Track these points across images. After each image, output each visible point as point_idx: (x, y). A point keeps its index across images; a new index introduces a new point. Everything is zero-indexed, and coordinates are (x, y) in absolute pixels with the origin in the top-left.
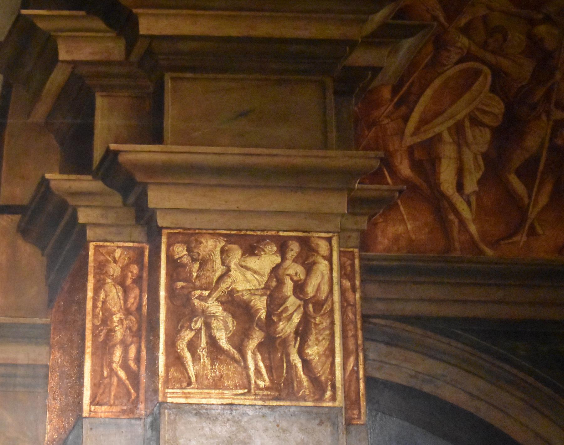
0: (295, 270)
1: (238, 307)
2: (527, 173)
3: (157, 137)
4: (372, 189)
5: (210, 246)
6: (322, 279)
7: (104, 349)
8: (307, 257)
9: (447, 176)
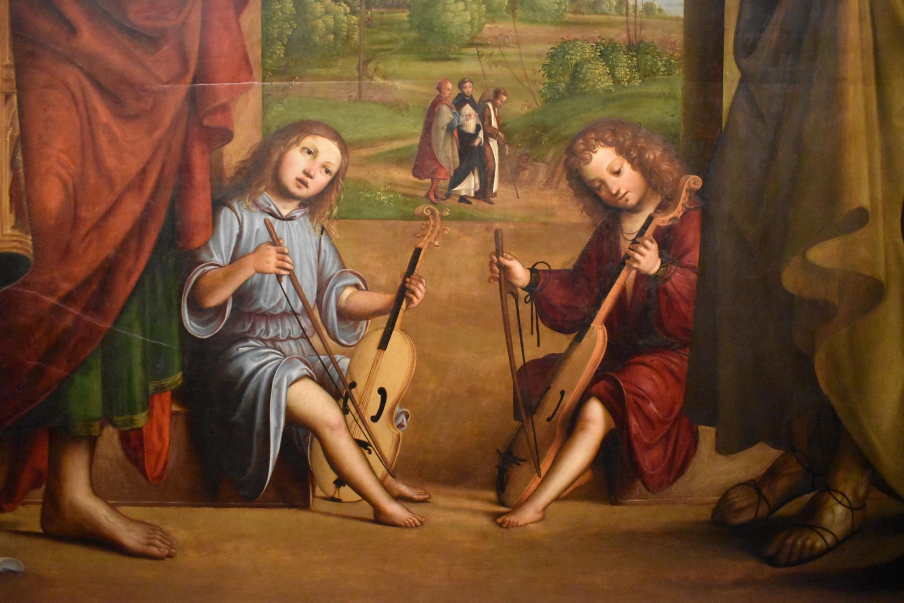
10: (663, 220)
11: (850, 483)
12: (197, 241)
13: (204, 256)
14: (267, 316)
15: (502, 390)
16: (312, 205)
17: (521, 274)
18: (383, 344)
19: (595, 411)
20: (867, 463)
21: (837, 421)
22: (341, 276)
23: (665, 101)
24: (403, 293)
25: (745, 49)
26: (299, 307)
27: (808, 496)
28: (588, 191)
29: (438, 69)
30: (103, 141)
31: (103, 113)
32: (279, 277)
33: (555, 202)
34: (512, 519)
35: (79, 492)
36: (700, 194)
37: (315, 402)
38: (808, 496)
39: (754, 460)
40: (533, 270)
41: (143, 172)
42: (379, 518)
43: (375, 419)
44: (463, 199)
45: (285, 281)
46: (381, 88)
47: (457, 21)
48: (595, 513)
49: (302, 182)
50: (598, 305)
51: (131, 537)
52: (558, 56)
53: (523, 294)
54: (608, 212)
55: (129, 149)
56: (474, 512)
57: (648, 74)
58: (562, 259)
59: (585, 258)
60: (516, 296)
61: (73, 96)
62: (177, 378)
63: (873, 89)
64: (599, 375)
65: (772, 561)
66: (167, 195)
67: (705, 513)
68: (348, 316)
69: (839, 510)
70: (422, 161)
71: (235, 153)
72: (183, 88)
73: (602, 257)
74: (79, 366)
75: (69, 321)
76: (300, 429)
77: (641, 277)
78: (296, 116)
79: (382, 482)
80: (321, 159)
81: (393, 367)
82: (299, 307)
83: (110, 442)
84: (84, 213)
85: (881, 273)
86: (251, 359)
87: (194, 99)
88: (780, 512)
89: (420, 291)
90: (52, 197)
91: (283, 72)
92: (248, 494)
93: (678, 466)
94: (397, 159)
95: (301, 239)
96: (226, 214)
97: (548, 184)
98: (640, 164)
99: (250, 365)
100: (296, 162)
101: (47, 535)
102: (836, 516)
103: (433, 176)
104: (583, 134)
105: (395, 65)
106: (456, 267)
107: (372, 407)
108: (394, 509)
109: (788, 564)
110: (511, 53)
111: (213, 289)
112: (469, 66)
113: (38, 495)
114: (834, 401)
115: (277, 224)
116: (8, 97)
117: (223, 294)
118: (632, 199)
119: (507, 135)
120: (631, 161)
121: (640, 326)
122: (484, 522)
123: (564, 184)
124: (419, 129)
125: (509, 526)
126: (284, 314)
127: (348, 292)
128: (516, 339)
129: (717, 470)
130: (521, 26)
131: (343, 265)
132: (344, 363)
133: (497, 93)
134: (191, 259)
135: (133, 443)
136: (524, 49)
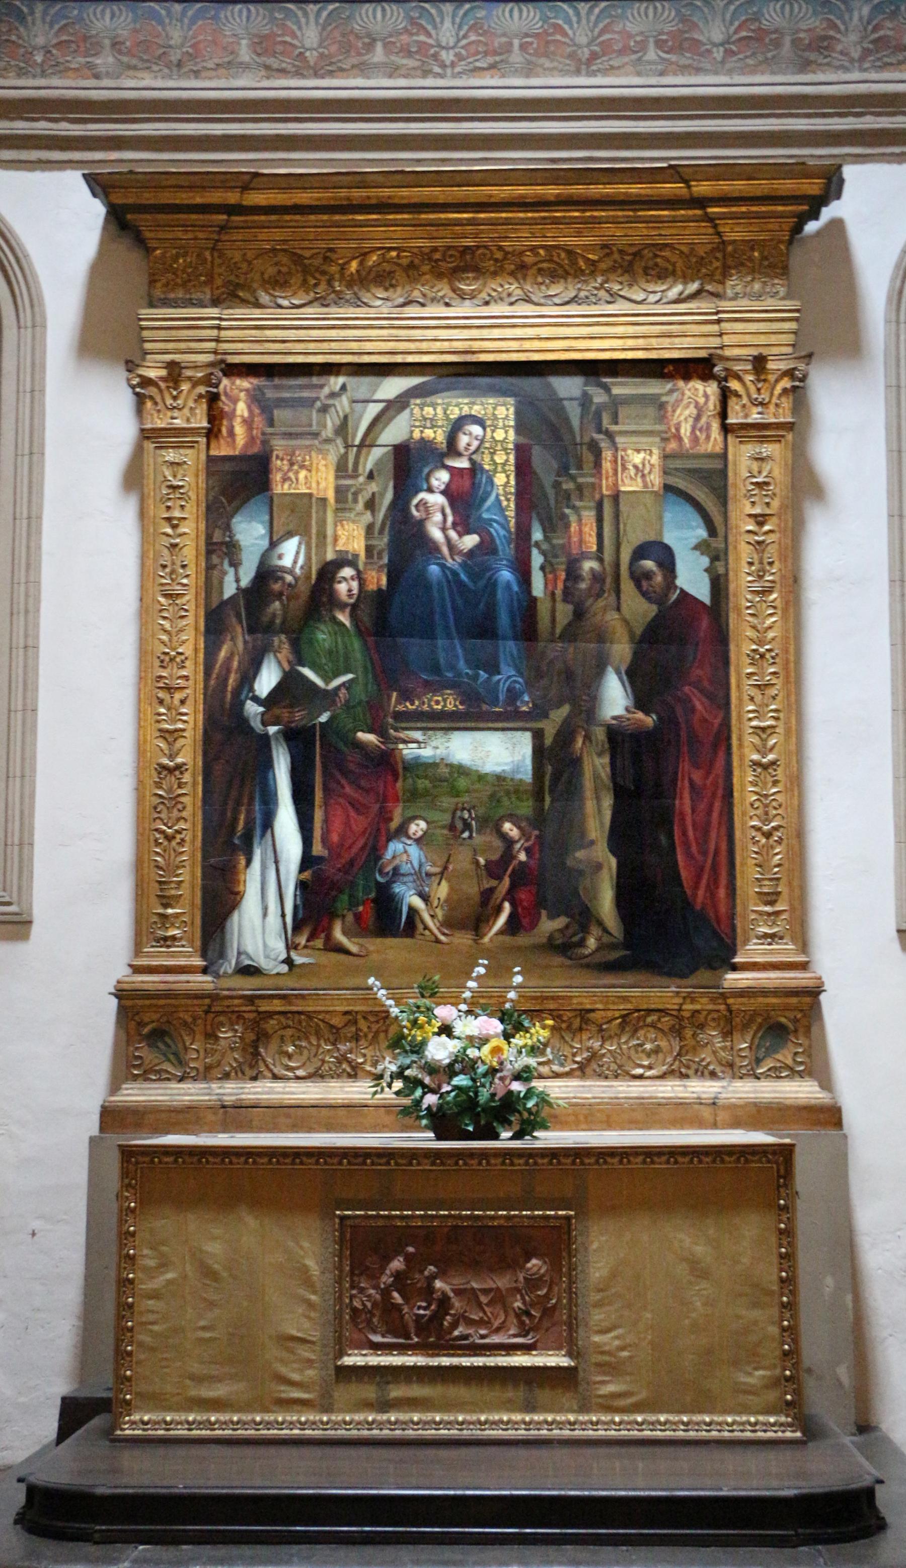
0: (648, 457)
1: (636, 467)
2: (701, 430)
3: (616, 423)
4: (664, 435)
5: (630, 452)
6: (655, 459)
7: (607, 478)
8: (651, 454)
9: (682, 431)
10: (526, 845)
11: (595, 931)
14: (403, 875)
15: (477, 899)
16: (418, 841)
17: (482, 861)
18: (439, 884)
19: (507, 905)
20: (600, 923)
23: (526, 808)
25: (551, 791)
28: (504, 837)
29: (456, 800)
31: (352, 814)
35: (338, 935)
36: (537, 837)
37: (417, 902)
39: (560, 922)
41: (364, 833)
42: (438, 941)
48: (507, 939)
51: (354, 949)
52: (492, 796)
55: (359, 823)
58: (495, 857)
65: (571, 959)
67: (544, 940)
68: (428, 875)
70: (452, 827)
71: (394, 825)
72: (378, 806)
73: (508, 854)
74: (341, 891)
76: (412, 911)
77: (521, 862)
81: (442, 890)
83: (350, 918)
86: (398, 888)
89: (451, 867)
90: (335, 838)
91: (408, 801)
93: (534, 924)
94: (443, 827)
95: (414, 852)
98: (519, 828)
101: (325, 949)
102: (592, 943)
105: (444, 799)
106: (462, 860)
108: (442, 938)
112: (466, 798)
113: (323, 935)
117: (389, 868)
118: (517, 838)
119: (476, 819)
121: (521, 876)
122: (470, 942)
129: (549, 925)
134: (379, 858)
135: (358, 917)
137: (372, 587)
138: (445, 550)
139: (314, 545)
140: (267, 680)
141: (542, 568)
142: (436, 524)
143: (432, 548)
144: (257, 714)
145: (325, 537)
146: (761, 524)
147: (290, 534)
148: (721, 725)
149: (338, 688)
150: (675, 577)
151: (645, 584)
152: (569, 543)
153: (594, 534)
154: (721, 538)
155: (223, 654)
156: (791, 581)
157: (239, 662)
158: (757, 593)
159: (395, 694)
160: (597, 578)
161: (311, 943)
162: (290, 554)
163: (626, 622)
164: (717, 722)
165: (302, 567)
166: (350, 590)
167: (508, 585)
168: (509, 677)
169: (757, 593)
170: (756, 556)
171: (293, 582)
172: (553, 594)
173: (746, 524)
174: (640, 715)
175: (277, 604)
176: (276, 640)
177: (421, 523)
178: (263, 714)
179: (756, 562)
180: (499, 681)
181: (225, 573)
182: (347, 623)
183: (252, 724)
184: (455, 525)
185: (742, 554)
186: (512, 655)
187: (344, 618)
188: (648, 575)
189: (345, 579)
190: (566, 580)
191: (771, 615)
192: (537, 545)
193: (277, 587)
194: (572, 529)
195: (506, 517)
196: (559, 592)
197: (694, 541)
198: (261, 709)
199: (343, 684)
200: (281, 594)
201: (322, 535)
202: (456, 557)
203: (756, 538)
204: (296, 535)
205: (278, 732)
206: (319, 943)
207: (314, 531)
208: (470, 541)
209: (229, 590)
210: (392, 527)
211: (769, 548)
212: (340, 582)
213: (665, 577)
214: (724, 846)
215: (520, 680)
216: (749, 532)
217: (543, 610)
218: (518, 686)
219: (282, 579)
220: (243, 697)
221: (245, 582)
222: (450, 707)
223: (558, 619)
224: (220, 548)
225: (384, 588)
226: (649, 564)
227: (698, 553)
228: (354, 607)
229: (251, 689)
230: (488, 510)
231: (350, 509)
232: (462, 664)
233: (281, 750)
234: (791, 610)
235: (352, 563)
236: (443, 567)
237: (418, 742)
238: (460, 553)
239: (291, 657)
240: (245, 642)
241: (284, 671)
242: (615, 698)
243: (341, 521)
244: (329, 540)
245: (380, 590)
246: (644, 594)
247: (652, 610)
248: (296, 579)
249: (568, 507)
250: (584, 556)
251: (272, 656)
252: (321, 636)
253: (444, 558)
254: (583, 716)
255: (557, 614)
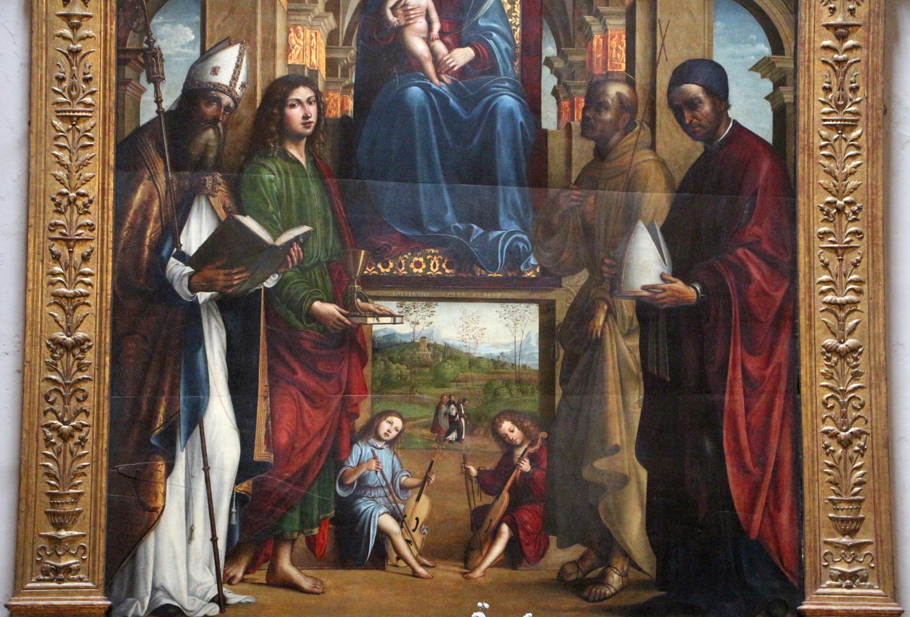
10: (531, 450)
11: (620, 564)
12: (343, 458)
13: (346, 463)
14: (372, 488)
15: (467, 519)
16: (391, 443)
17: (473, 471)
18: (418, 500)
19: (505, 528)
20: (627, 555)
21: (611, 536)
22: (401, 472)
23: (531, 403)
24: (426, 479)
25: (564, 382)
26: (384, 484)
27: (600, 569)
28: (501, 439)
29: (440, 391)
30: (306, 416)
32: (376, 472)
33: (487, 443)
34: (471, 575)
35: (286, 565)
37: (389, 523)
38: (600, 569)
40: (478, 470)
41: (322, 430)
42: (415, 574)
43: (414, 530)
44: (450, 441)
45: (379, 474)
46: (419, 398)
47: (448, 372)
48: (505, 573)
49: (386, 434)
50: (505, 484)
51: (306, 584)
52: (487, 387)
53: (474, 479)
54: (509, 447)
55: (316, 419)
56: (454, 571)
57: (524, 393)
58: (490, 466)
59: (500, 464)
60: (472, 480)
61: (294, 399)
62: (332, 513)
63: (620, 397)
64: (505, 514)
65: (587, 599)
66: (331, 440)
67: (554, 575)
68: (404, 488)
69: (616, 576)
70: (435, 427)
71: (360, 422)
72: (340, 396)
73: (507, 463)
74: (291, 508)
75: (287, 489)
76: (383, 535)
77: (523, 473)
78: (387, 408)
79: (416, 558)
80: (394, 425)
81: (422, 508)
82: (384, 484)
83: (301, 542)
84: (296, 445)
85: (627, 472)
86: (364, 505)
87: (343, 400)
88: (588, 576)
90: (283, 438)
92: (360, 564)
93: (541, 553)
94: (426, 427)
95: (386, 457)
96: (356, 446)
97: (484, 436)
98: (521, 428)
99: (363, 508)
100: (384, 427)
101: (268, 584)
102: (615, 579)
103: (439, 432)
104: (498, 416)
106: (447, 470)
107: (413, 526)
108: (421, 570)
109: (594, 601)
110: (469, 385)
111: (350, 476)
112: (453, 389)
113: (266, 566)
114: (608, 525)
115: (376, 451)
116: (265, 398)
117: (354, 478)
118: (519, 441)
119: (468, 416)
120: (518, 427)
121: (523, 491)
122: (459, 576)
123: (491, 436)
124: (433, 414)
125: (470, 578)
126: (378, 487)
127: (404, 478)
128: (472, 498)
129: (559, 556)
130: (473, 374)
131: (402, 467)
132: (402, 507)
133: (464, 400)
134: (340, 464)
135: (311, 542)
136: (476, 383)
137: (335, 113)
138: (430, 68)
139: (259, 57)
140: (197, 232)
141: (555, 93)
142: (418, 32)
143: (412, 64)
144: (181, 277)
145: (274, 47)
146: (842, 38)
147: (227, 42)
148: (784, 297)
149: (290, 244)
150: (728, 106)
151: (688, 115)
152: (591, 61)
153: (623, 49)
154: (788, 55)
155: (138, 197)
156: (880, 112)
157: (160, 206)
158: (835, 128)
159: (363, 252)
160: (625, 106)
161: (246, 577)
162: (227, 66)
163: (662, 163)
164: (779, 295)
165: (243, 86)
166: (306, 117)
167: (511, 114)
168: (512, 233)
169: (835, 128)
170: (834, 80)
171: (232, 105)
172: (569, 127)
173: (822, 38)
174: (679, 285)
175: (211, 133)
176: (209, 181)
177: (399, 31)
178: (191, 276)
179: (835, 89)
180: (500, 236)
181: (142, 91)
182: (302, 160)
183: (177, 288)
184: (442, 34)
185: (817, 77)
186: (514, 204)
187: (297, 152)
188: (692, 104)
189: (299, 102)
190: (585, 110)
191: (853, 157)
192: (549, 62)
193: (211, 110)
194: (595, 43)
195: (509, 25)
196: (576, 124)
197: (754, 60)
198: (189, 269)
199: (296, 239)
200: (216, 120)
201: (270, 46)
202: (444, 77)
203: (836, 56)
204: (236, 43)
205: (211, 299)
206: (260, 576)
207: (259, 38)
208: (463, 56)
209: (148, 113)
210: (361, 37)
211: (853, 68)
212: (293, 106)
213: (714, 105)
214: (787, 456)
215: (525, 237)
216: (826, 48)
217: (556, 145)
218: (521, 245)
219: (218, 100)
220: (165, 253)
221: (167, 105)
222: (434, 271)
223: (574, 161)
224: (137, 58)
225: (350, 114)
226: (694, 89)
227: (758, 75)
228: (311, 140)
229: (176, 243)
230: (486, 15)
231: (307, 12)
232: (449, 215)
233: (214, 323)
234: (880, 152)
235: (309, 81)
236: (426, 89)
237: (391, 315)
238: (449, 71)
239: (228, 202)
240: (168, 182)
241: (219, 219)
242: (647, 263)
243: (296, 26)
244: (280, 51)
245: (345, 117)
246: (687, 129)
247: (697, 149)
248: (236, 101)
249: (589, 14)
250: (609, 78)
251: (203, 201)
252: (267, 176)
253: (427, 77)
254: (606, 285)
255: (573, 153)
